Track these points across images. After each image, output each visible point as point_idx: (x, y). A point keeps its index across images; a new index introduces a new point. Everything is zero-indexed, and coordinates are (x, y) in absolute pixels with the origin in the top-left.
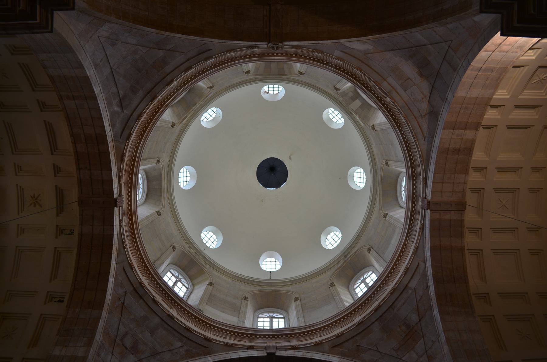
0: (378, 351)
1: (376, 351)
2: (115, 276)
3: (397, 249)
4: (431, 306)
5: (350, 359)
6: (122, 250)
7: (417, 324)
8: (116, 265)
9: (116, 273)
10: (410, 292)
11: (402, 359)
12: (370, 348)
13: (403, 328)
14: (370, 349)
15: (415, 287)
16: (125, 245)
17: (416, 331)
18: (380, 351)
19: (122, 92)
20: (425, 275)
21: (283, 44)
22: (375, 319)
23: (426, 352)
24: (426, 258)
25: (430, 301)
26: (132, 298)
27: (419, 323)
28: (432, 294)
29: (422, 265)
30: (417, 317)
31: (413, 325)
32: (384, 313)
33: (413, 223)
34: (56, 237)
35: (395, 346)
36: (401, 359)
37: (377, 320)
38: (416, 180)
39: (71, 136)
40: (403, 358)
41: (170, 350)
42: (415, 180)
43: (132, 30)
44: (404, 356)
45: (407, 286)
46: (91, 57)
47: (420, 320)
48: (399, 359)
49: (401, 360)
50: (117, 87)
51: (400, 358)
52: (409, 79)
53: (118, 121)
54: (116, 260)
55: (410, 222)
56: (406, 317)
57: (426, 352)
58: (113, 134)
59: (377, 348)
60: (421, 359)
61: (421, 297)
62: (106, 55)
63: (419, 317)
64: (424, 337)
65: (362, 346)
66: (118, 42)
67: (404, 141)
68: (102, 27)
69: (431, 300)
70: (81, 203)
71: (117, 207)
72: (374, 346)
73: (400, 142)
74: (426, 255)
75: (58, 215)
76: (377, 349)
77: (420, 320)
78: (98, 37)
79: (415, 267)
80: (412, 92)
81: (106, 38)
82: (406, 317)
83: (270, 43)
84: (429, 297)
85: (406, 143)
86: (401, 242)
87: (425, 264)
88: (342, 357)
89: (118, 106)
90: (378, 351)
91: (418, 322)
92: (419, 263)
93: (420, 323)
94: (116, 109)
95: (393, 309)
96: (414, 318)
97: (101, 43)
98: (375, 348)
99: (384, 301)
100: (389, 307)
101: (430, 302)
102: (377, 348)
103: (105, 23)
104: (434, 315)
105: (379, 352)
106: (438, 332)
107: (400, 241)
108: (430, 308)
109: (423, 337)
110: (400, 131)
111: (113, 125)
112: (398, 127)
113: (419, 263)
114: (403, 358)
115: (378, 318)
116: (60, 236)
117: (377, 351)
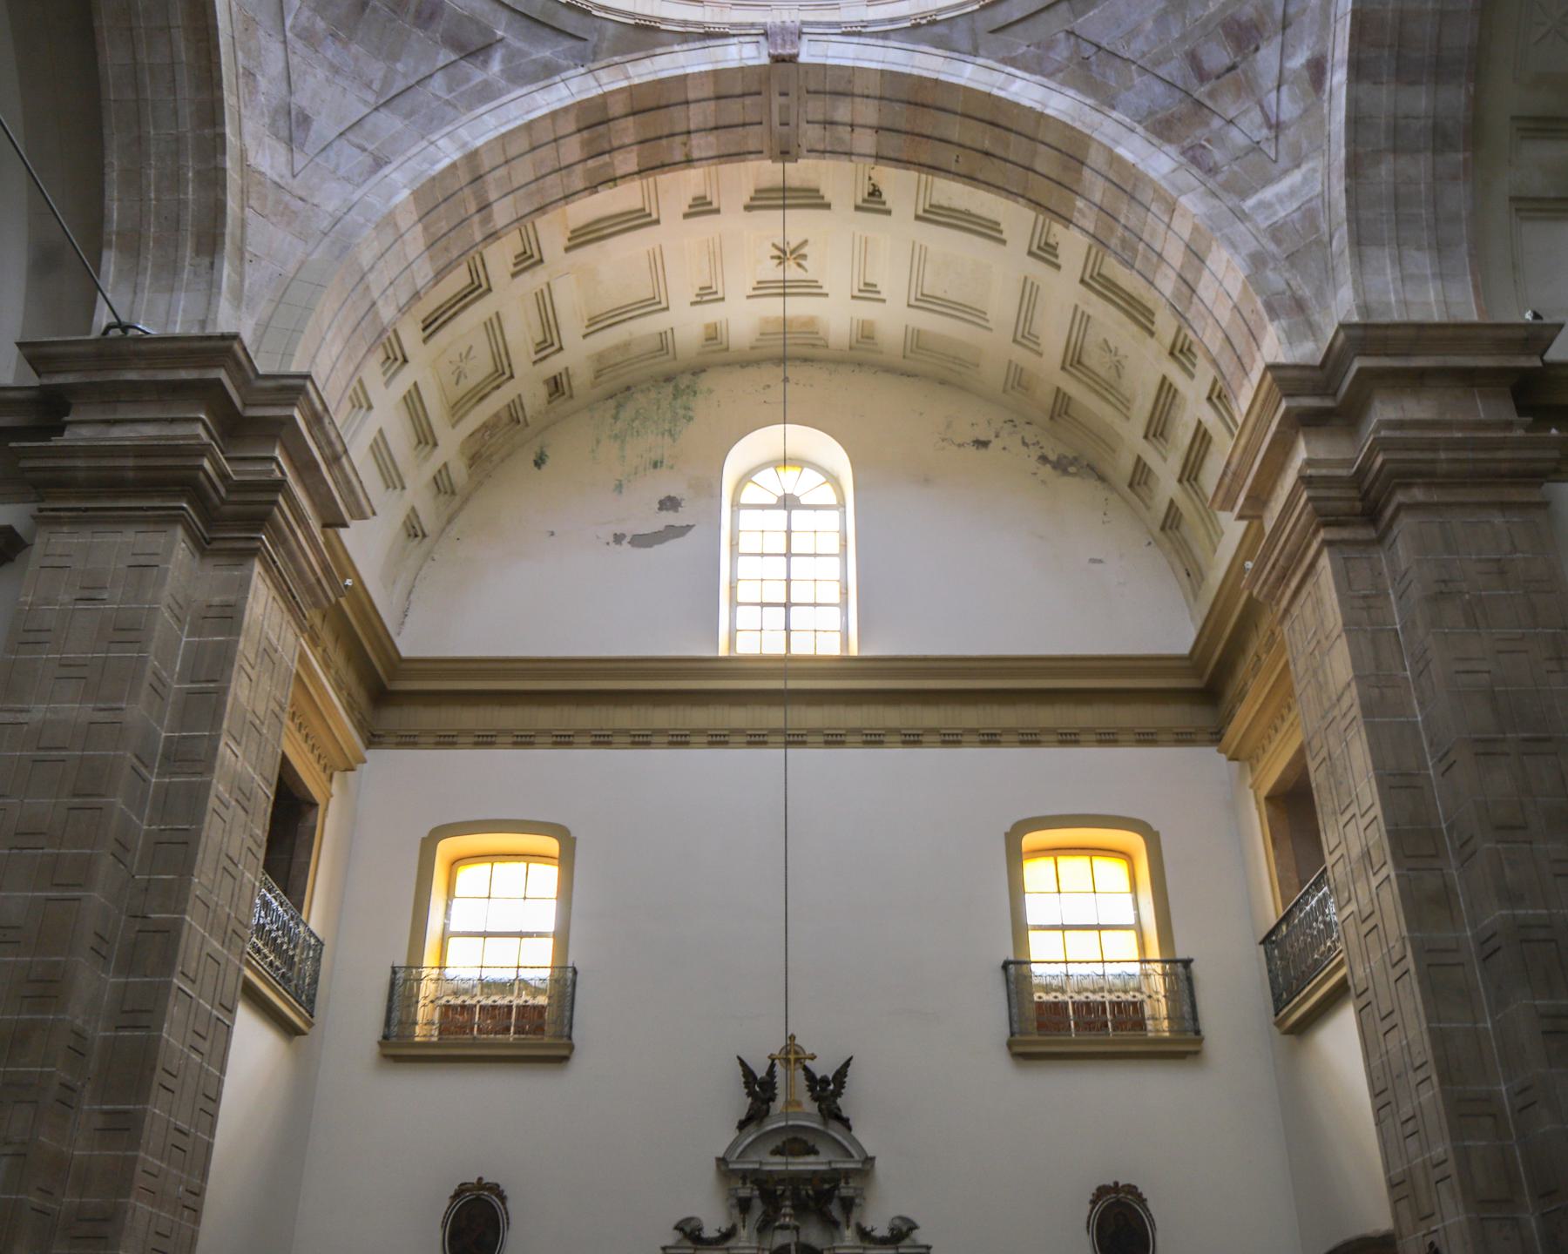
2: (1013, 66)
6: (940, 30)
8: (980, 61)
9: (1004, 61)
16: (925, 17)
19: (441, 57)
26: (1091, 14)
34: (888, 212)
39: (597, 192)
43: (244, 68)
46: (358, 186)
50: (431, 76)
53: (533, 57)
54: (962, 57)
58: (576, 66)
62: (341, 134)
66: (292, 106)
68: (262, 174)
70: (785, 154)
71: (796, 56)
75: (828, 206)
78: (294, 176)
81: (292, 150)
89: (485, 63)
94: (496, 66)
97: (312, 160)
103: (249, 166)
111: (547, 72)
116: (884, 203)
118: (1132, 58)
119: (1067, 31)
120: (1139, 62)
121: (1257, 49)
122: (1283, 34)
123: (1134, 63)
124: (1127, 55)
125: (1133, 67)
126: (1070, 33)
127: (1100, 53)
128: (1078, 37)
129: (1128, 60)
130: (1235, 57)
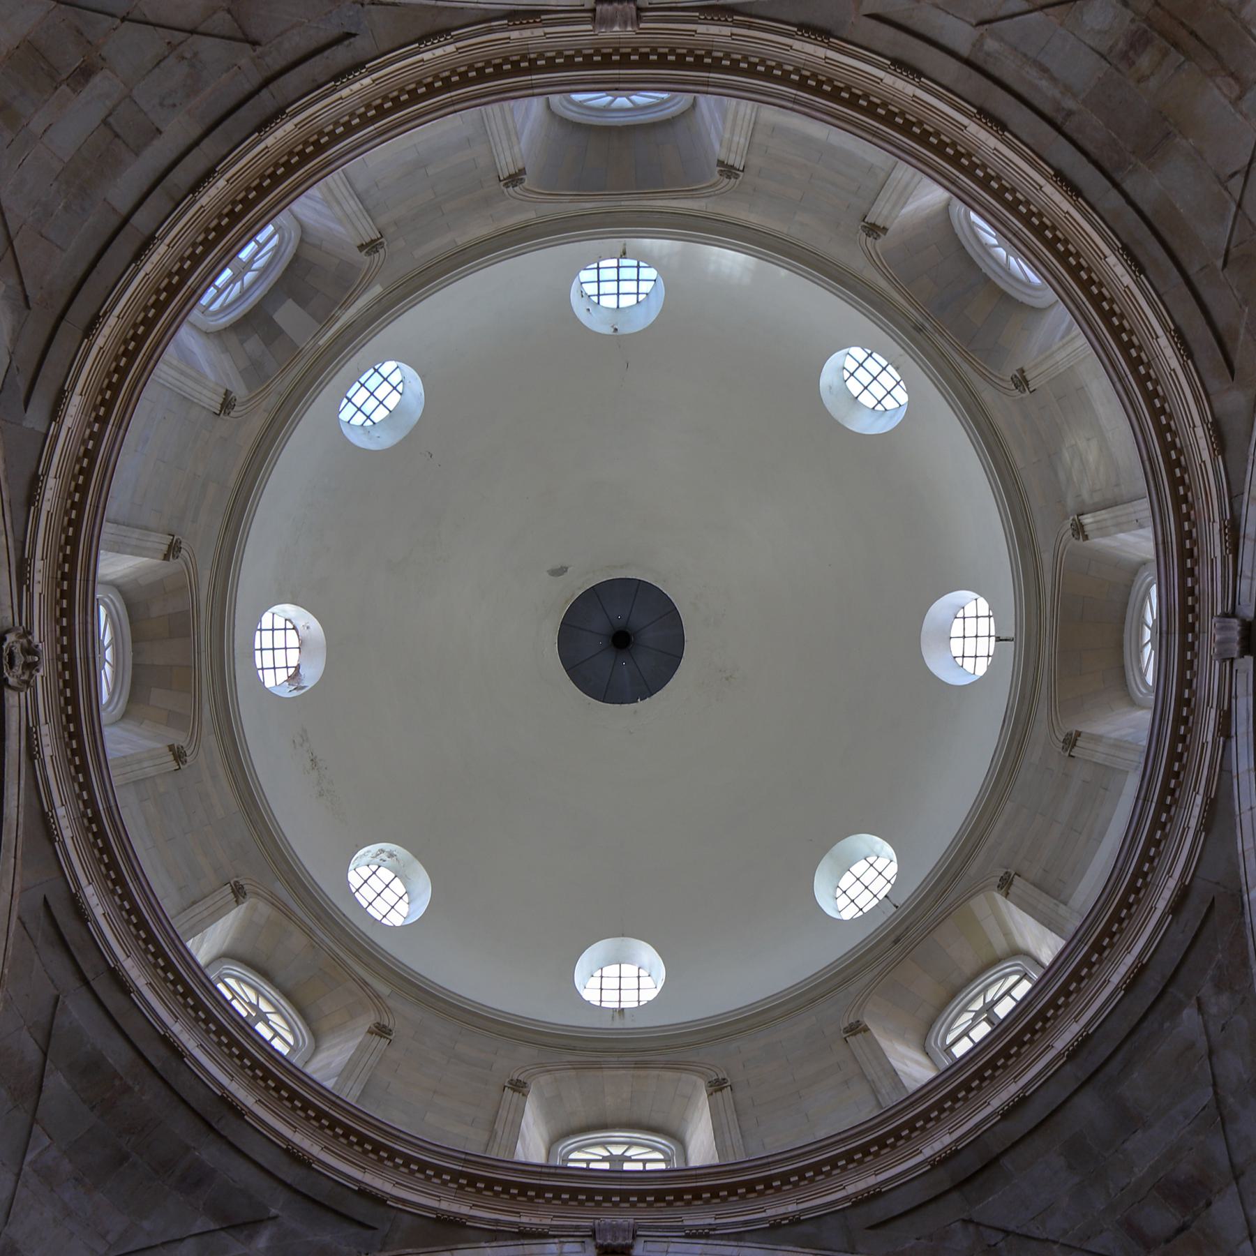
3: (825, 117)
12: (1234, 208)
13: (1145, 61)
15: (972, 25)
21: (8, 631)
22: (1114, 193)
31: (1133, 21)
33: (709, 53)
37: (1116, 185)
38: (532, 56)
41: (1211, 1053)
42: (530, 60)
52: (111, 120)
55: (708, 68)
56: (1098, 53)
67: (373, 120)
72: (1226, 189)
73: (384, 134)
79: (888, 32)
80: (161, 105)
82: (1098, 53)
83: (6, 679)
85: (382, 113)
86: (795, 101)
95: (1070, 113)
99: (1038, 156)
107: (790, 105)
110: (335, 139)
112: (320, 148)
117: (1247, 173)
118: (1051, 1237)
119: (964, 1220)
120: (1061, 1241)
121: (1209, 1204)
122: (1237, 1183)
123: (1055, 1242)
124: (1045, 1236)
125: (1055, 1247)
126: (967, 1222)
127: (1010, 1237)
128: (978, 1224)
129: (1047, 1240)
130: (1183, 1217)
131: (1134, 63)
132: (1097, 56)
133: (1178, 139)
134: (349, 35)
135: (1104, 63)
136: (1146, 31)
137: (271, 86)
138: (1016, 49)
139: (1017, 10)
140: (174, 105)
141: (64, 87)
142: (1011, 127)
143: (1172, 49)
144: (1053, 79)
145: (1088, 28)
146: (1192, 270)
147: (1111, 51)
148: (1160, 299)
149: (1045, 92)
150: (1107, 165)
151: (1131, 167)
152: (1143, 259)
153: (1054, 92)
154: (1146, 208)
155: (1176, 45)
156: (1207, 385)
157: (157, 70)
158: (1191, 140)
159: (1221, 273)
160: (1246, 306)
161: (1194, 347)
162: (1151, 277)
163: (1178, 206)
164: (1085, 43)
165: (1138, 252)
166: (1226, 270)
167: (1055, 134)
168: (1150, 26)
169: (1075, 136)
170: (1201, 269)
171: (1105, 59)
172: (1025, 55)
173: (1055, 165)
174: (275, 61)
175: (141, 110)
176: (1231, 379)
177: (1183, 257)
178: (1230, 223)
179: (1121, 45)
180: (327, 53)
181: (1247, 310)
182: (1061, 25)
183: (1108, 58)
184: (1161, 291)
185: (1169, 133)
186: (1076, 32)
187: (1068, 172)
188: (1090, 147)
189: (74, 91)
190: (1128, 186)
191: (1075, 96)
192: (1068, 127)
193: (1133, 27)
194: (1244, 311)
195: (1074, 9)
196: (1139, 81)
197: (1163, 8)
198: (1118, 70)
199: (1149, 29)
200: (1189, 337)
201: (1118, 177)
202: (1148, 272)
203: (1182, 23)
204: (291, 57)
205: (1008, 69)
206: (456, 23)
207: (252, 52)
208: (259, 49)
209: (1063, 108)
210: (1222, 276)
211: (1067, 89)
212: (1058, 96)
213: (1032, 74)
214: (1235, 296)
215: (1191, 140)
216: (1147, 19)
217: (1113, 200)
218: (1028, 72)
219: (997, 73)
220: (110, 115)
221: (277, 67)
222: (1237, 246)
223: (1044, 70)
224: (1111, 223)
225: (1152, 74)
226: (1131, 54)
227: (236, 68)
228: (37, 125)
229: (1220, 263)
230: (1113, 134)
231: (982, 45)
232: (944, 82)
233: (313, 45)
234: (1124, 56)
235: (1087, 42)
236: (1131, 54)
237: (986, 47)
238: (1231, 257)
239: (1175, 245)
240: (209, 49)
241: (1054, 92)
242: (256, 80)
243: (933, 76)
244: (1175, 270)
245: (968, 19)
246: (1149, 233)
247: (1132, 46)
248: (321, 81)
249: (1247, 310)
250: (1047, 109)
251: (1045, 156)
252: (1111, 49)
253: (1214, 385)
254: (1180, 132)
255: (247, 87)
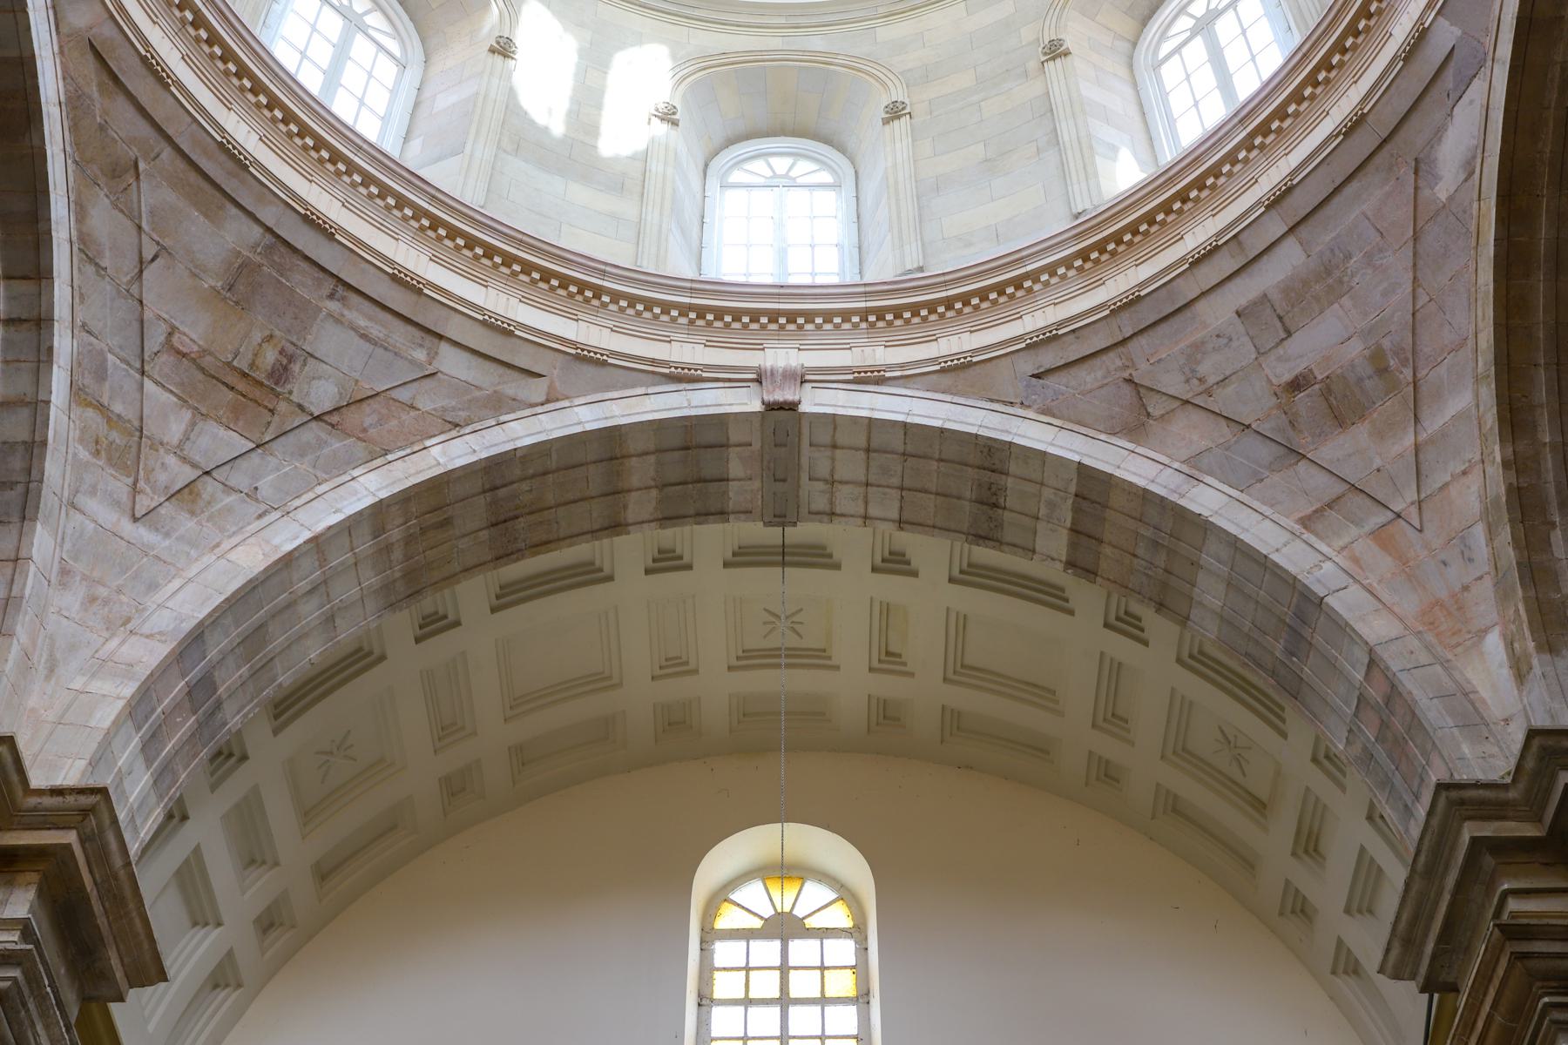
0: (142, 264)
1: (141, 253)
4: (387, 452)
5: (68, 149)
7: (300, 407)
10: (420, 355)
11: (145, 378)
12: (144, 225)
13: (270, 356)
14: (140, 228)
15: (442, 372)
17: (272, 411)
18: (145, 273)
20: (499, 405)
22: (270, 223)
23: (207, 473)
24: (566, 403)
25: (406, 447)
27: (310, 418)
28: (435, 451)
29: (536, 390)
30: (328, 406)
31: (290, 392)
32: (307, 258)
35: (185, 334)
36: (143, 373)
37: (269, 230)
40: (149, 385)
44: (157, 383)
45: (441, 337)
47: (318, 418)
48: (138, 365)
49: (138, 376)
51: (146, 368)
56: (316, 358)
57: (207, 473)
59: (153, 260)
60: (171, 460)
61: (412, 407)
63: (330, 412)
64: (259, 451)
65: (139, 187)
69: (408, 451)
72: (158, 243)
74: (577, 401)
76: (150, 257)
77: (318, 418)
82: (316, 358)
84: (415, 439)
87: (542, 404)
88: (64, 107)
90: (142, 264)
91: (312, 414)
92: (541, 376)
93: (310, 420)
95: (331, 296)
96: (322, 394)
98: (148, 253)
99: (355, 250)
100: (332, 275)
101: (401, 448)
102: (153, 260)
104: (356, 473)
105: (141, 271)
106: (297, 503)
107: (608, 269)
108: (377, 452)
109: (258, 446)
113: (541, 376)
114: (149, 385)
115: (278, 237)
131: (281, 353)
132: (317, 355)
133: (219, 284)
134: (1037, 376)
135: (309, 349)
136: (276, 384)
137: (1121, 339)
138: (396, 354)
139: (400, 389)
140: (1218, 336)
141: (1320, 377)
142: (386, 278)
143: (247, 371)
144: (354, 328)
145: (330, 380)
146: (167, 153)
147: (304, 360)
148: (195, 116)
149: (359, 315)
150: (283, 249)
151: (259, 251)
152: (223, 158)
153: (350, 315)
154: (234, 211)
155: (245, 375)
156: (116, 30)
157: (1227, 373)
158: (206, 286)
159: (138, 154)
160: (100, 124)
161: (143, 71)
162: (209, 139)
163: (202, 218)
164: (331, 366)
165: (230, 165)
166: (133, 158)
167: (342, 276)
168: (272, 389)
169: (321, 275)
170: (158, 156)
171: (308, 353)
172: (386, 349)
173: (335, 244)
174: (1113, 360)
175: (1252, 339)
176: (92, 39)
177: (181, 164)
178: (143, 209)
179: (296, 367)
180: (1062, 362)
181: (98, 119)
182: (357, 381)
183: (306, 355)
184: (194, 126)
185: (229, 289)
186: (341, 374)
187: (322, 240)
188: (304, 265)
189: (1311, 370)
190: (257, 231)
191: (330, 315)
192: (329, 284)
193: (289, 387)
194: (100, 117)
195: (348, 396)
196: (271, 336)
197: (266, 407)
198: (292, 343)
199: (273, 386)
200: (151, 80)
201: (269, 238)
202: (213, 145)
203: (244, 396)
204: (1097, 362)
205: (400, 335)
206: (934, 377)
207: (1134, 373)
208: (1126, 375)
209: (339, 300)
210: (135, 149)
211: (338, 321)
212: (346, 312)
213: (376, 331)
214: (116, 133)
215: (206, 286)
216: (277, 395)
217: (268, 215)
218: (380, 332)
219: (410, 328)
220: (1283, 340)
221: (1112, 354)
222: (129, 185)
223: (364, 337)
224: (265, 190)
225: (260, 345)
226: (285, 361)
227: (1152, 362)
228: (1356, 349)
229: (142, 166)
230: (284, 281)
231: (428, 354)
232: (459, 316)
233: (1074, 371)
234: (291, 359)
235: (328, 367)
236: (285, 361)
237: (425, 352)
238: (132, 171)
239: (193, 177)
240: (1173, 383)
241: (350, 315)
242: (1133, 346)
243: (471, 321)
244: (187, 151)
245: (446, 377)
246: (223, 186)
247: (285, 368)
248: (1071, 337)
249: (98, 119)
250: (354, 299)
251: (347, 252)
252: (305, 364)
253: (108, 30)
254: (219, 292)
255: (1143, 341)
